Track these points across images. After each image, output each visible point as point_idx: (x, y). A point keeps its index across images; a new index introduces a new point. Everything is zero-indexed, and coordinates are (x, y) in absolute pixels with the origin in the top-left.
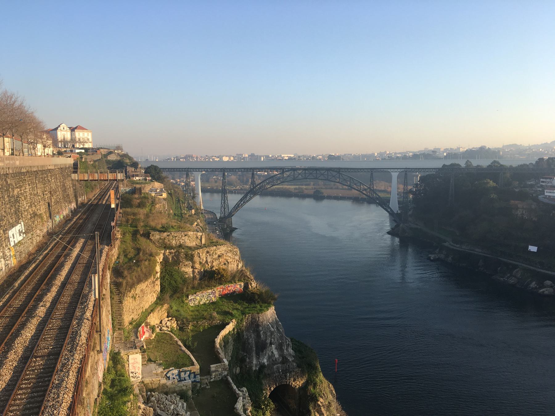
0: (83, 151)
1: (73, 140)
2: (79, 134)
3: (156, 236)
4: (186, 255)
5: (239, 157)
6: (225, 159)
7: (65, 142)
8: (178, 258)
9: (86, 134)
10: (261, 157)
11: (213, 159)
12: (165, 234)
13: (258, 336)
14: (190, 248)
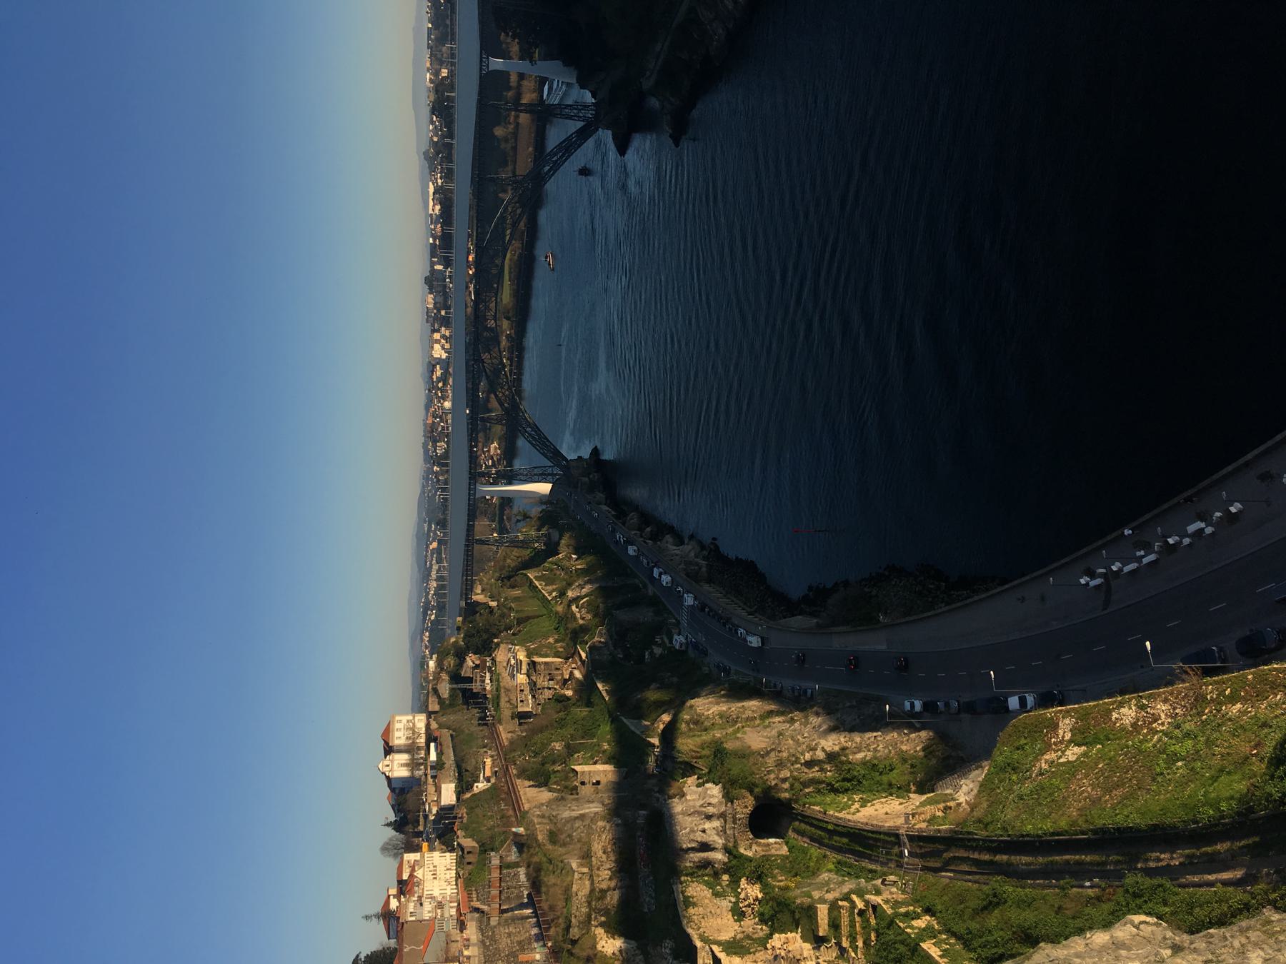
0: (432, 745)
1: (410, 749)
2: (399, 738)
3: (575, 932)
4: (599, 899)
5: (437, 320)
6: (439, 352)
7: (413, 765)
8: (600, 910)
9: (397, 726)
10: (433, 271)
11: (439, 380)
12: (573, 920)
13: (692, 849)
14: (592, 891)
